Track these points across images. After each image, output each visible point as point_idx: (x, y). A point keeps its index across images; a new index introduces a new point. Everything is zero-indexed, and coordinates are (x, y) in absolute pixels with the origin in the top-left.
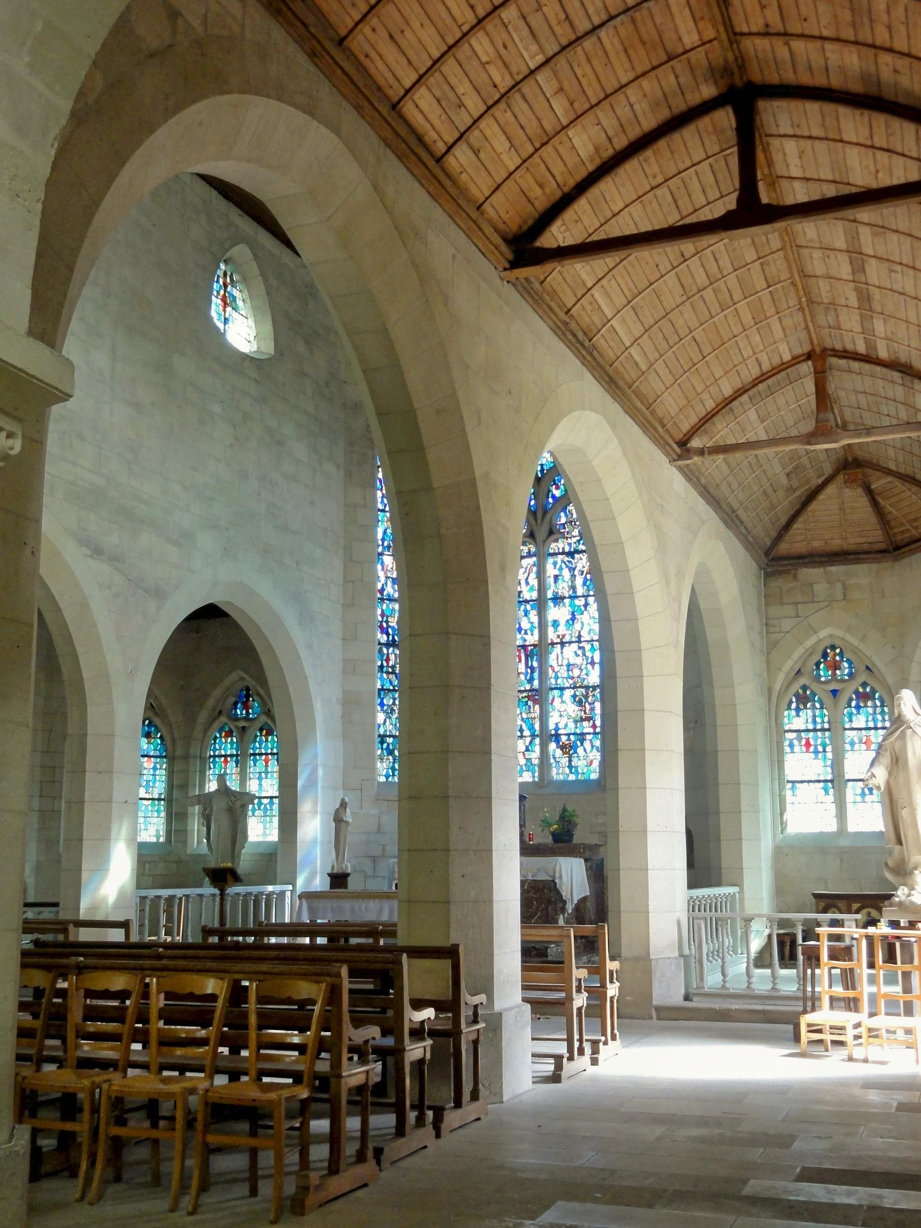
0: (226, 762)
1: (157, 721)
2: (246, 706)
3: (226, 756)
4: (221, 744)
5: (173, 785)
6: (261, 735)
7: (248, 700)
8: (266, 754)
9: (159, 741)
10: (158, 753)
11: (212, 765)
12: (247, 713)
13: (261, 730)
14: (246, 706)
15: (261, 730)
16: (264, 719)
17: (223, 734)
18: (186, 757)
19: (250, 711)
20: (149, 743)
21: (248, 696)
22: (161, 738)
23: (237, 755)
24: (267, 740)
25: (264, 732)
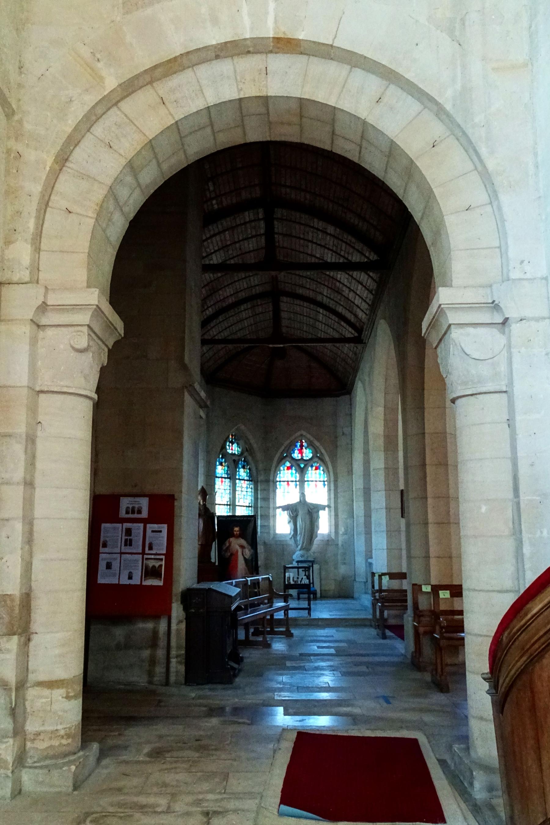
0: (288, 484)
1: (250, 458)
2: (301, 452)
3: (288, 482)
4: (284, 474)
5: (257, 498)
6: (312, 470)
7: (302, 449)
8: (316, 481)
9: (248, 471)
10: (248, 478)
11: (278, 486)
12: (302, 455)
13: (312, 466)
14: (301, 452)
15: (312, 466)
16: (316, 459)
17: (286, 468)
18: (267, 481)
19: (304, 455)
20: (244, 472)
21: (302, 446)
22: (249, 469)
23: (296, 481)
24: (316, 473)
25: (314, 468)
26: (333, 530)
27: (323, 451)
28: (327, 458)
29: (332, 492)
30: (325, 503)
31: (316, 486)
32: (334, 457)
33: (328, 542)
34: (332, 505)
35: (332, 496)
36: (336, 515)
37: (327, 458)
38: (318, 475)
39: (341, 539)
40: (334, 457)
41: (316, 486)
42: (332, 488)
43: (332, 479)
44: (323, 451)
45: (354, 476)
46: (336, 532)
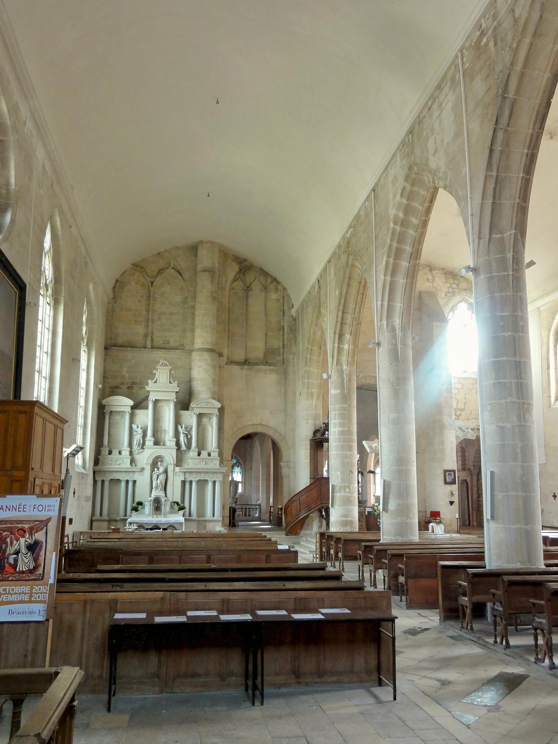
16: (238, 463)
26: (244, 491)
27: (241, 461)
28: (242, 463)
29: (244, 476)
30: (241, 481)
31: (237, 473)
32: (245, 462)
33: (241, 495)
34: (244, 481)
35: (244, 478)
36: (245, 485)
37: (242, 463)
38: (238, 470)
39: (246, 494)
40: (245, 462)
41: (237, 473)
42: (244, 474)
43: (244, 471)
44: (241, 461)
45: (252, 471)
46: (245, 491)
